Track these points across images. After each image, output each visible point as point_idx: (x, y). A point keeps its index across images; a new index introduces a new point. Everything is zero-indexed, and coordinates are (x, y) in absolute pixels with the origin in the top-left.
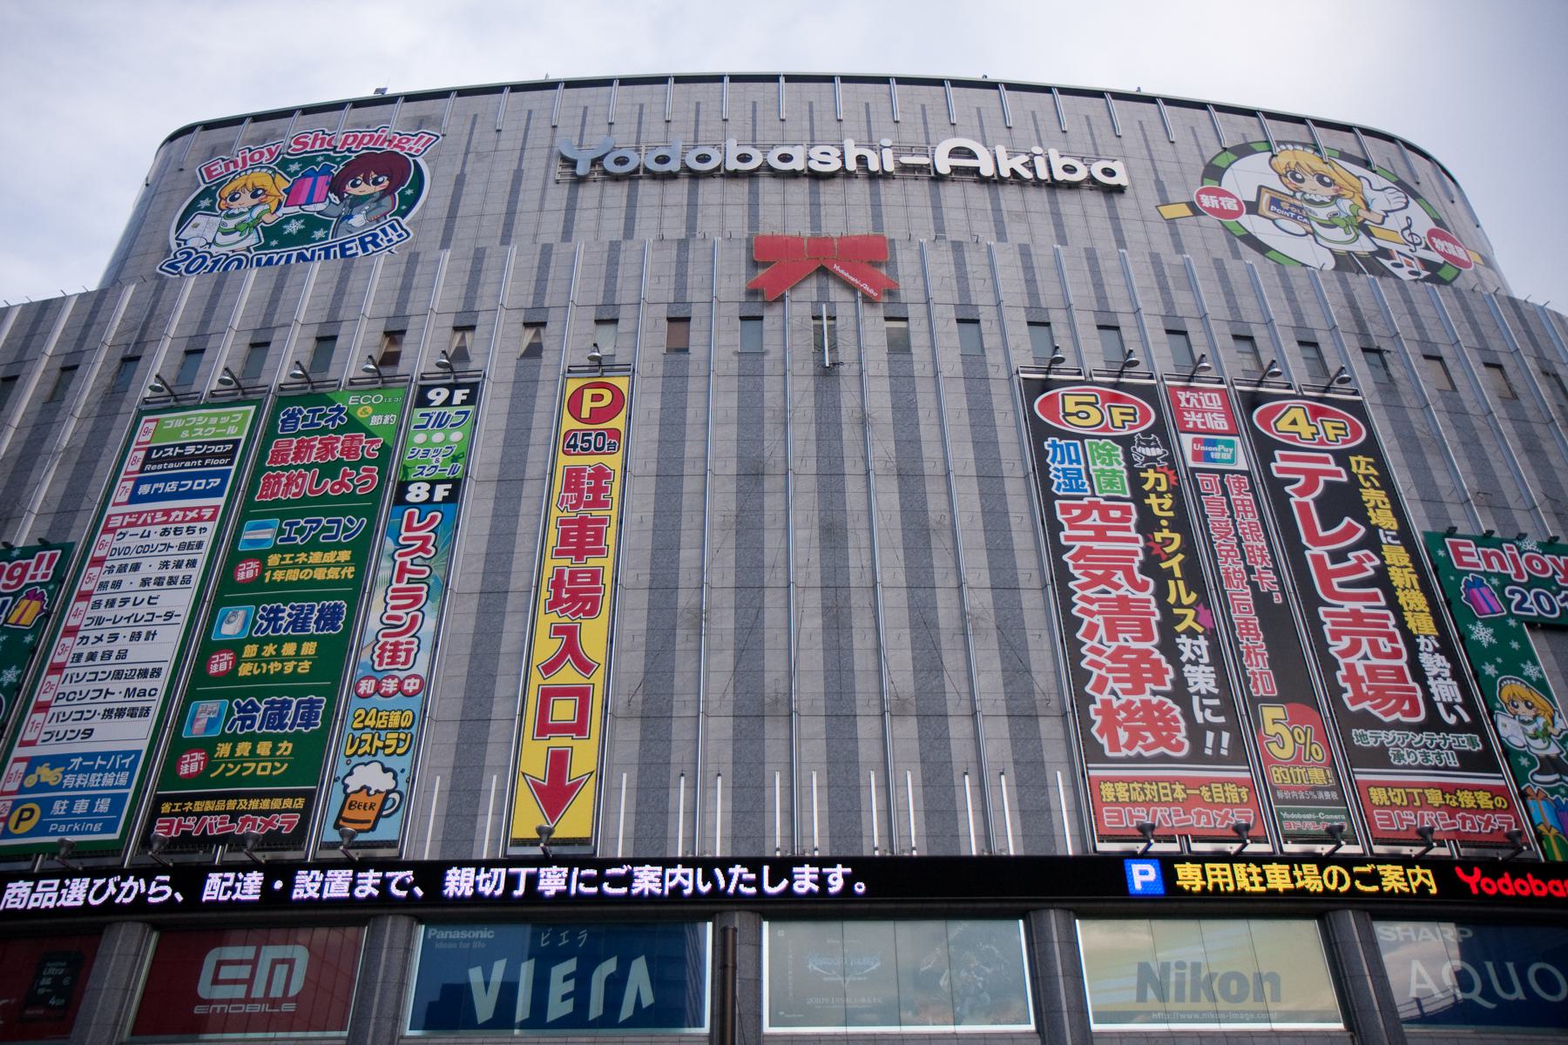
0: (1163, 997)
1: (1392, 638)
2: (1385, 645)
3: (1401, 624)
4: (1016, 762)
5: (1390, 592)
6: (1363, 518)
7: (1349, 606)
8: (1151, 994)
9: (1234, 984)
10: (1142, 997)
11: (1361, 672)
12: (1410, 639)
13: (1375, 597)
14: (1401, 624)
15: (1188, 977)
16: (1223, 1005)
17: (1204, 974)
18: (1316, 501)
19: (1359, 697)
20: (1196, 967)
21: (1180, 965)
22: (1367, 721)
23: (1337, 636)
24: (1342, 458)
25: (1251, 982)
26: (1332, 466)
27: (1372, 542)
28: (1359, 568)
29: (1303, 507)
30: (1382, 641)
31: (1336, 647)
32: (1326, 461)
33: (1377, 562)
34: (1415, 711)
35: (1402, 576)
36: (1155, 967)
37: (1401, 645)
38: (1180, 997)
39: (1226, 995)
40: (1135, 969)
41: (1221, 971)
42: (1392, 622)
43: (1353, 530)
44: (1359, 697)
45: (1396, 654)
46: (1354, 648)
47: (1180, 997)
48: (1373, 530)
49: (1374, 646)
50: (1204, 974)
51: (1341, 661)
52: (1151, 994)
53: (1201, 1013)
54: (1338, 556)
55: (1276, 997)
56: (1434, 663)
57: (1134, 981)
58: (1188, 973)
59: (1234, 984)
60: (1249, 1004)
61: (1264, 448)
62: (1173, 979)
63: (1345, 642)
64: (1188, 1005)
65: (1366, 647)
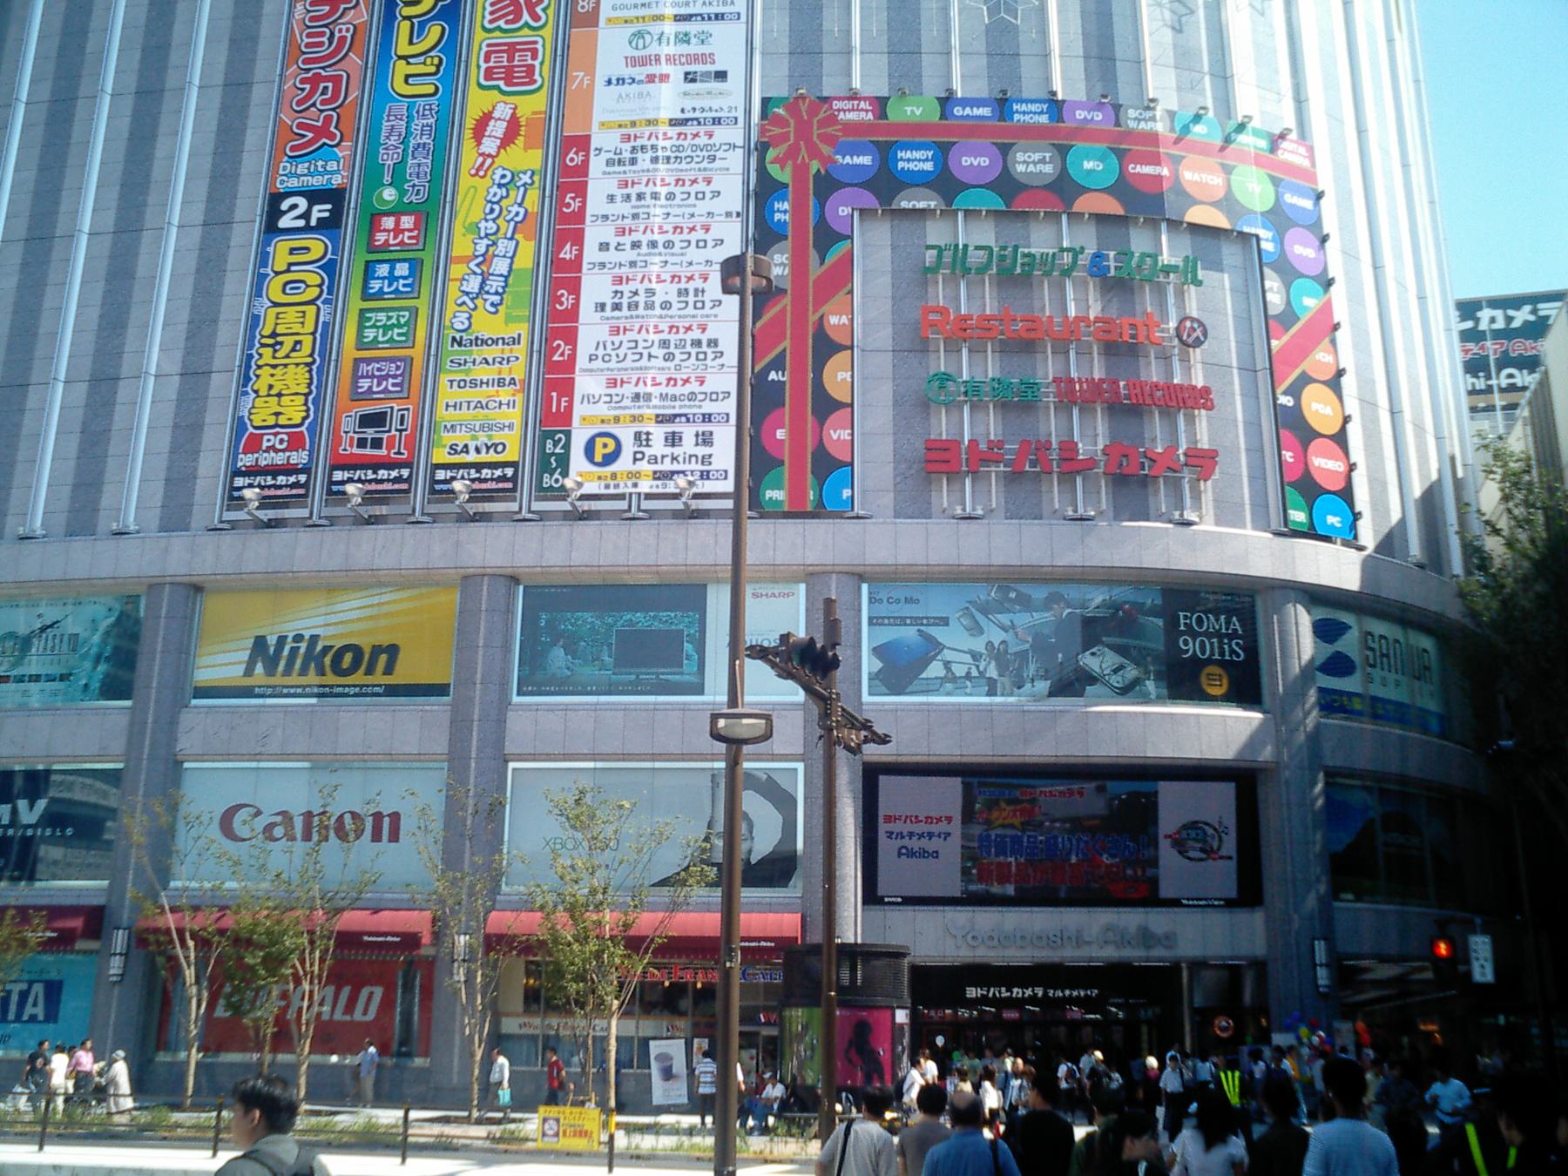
0: (270, 669)
4: (176, 426)
8: (259, 668)
9: (348, 659)
10: (249, 671)
15: (302, 650)
16: (331, 679)
17: (319, 648)
20: (314, 639)
21: (298, 638)
25: (367, 657)
36: (272, 640)
38: (288, 671)
39: (337, 669)
40: (250, 642)
41: (339, 644)
47: (288, 671)
50: (319, 648)
52: (259, 668)
53: (304, 687)
55: (389, 670)
57: (245, 655)
58: (303, 646)
59: (348, 659)
60: (359, 678)
62: (286, 652)
64: (295, 679)
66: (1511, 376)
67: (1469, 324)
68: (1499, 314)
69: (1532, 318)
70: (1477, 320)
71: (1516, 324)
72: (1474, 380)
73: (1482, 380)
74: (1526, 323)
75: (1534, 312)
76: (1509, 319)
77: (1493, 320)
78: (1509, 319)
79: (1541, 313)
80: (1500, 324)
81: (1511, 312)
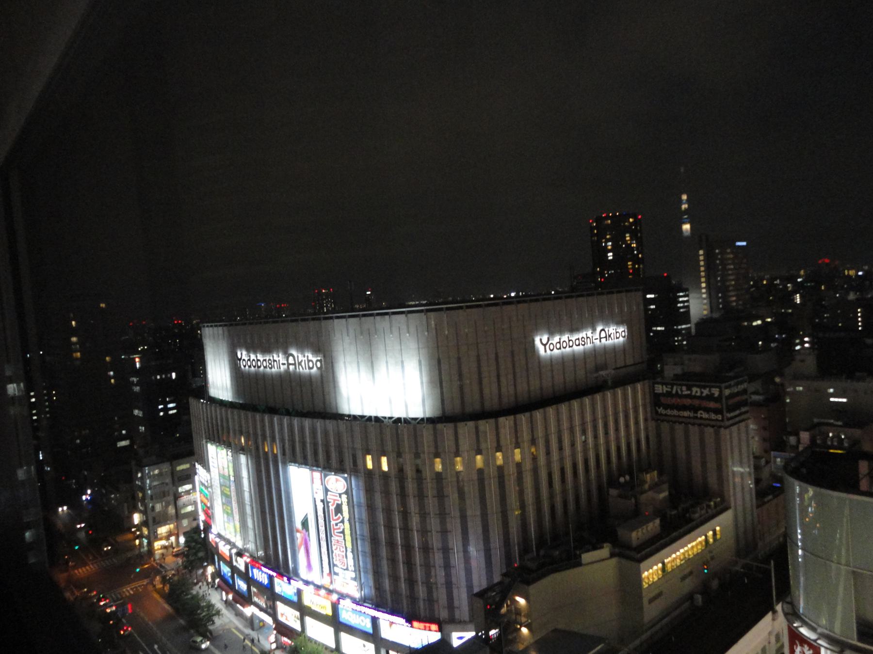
1: (343, 548)
2: (342, 550)
3: (345, 544)
5: (344, 535)
6: (342, 515)
7: (337, 538)
11: (337, 555)
12: (346, 548)
13: (341, 537)
14: (345, 544)
18: (335, 509)
19: (336, 560)
22: (336, 565)
23: (334, 545)
24: (340, 495)
26: (338, 498)
27: (343, 522)
28: (339, 529)
29: (332, 510)
30: (341, 548)
31: (334, 548)
32: (337, 496)
33: (343, 527)
34: (344, 566)
35: (348, 532)
37: (344, 549)
42: (344, 543)
43: (339, 518)
44: (336, 560)
45: (343, 552)
46: (336, 549)
48: (343, 518)
49: (340, 549)
51: (334, 551)
54: (336, 525)
56: (350, 555)
61: (326, 491)
63: (336, 546)
65: (338, 549)
66: (701, 414)
67: (689, 392)
68: (698, 390)
69: (709, 393)
70: (692, 391)
71: (704, 395)
72: (690, 413)
73: (692, 414)
74: (707, 395)
75: (710, 391)
76: (702, 393)
77: (697, 392)
78: (702, 393)
79: (712, 392)
80: (698, 394)
81: (702, 390)
